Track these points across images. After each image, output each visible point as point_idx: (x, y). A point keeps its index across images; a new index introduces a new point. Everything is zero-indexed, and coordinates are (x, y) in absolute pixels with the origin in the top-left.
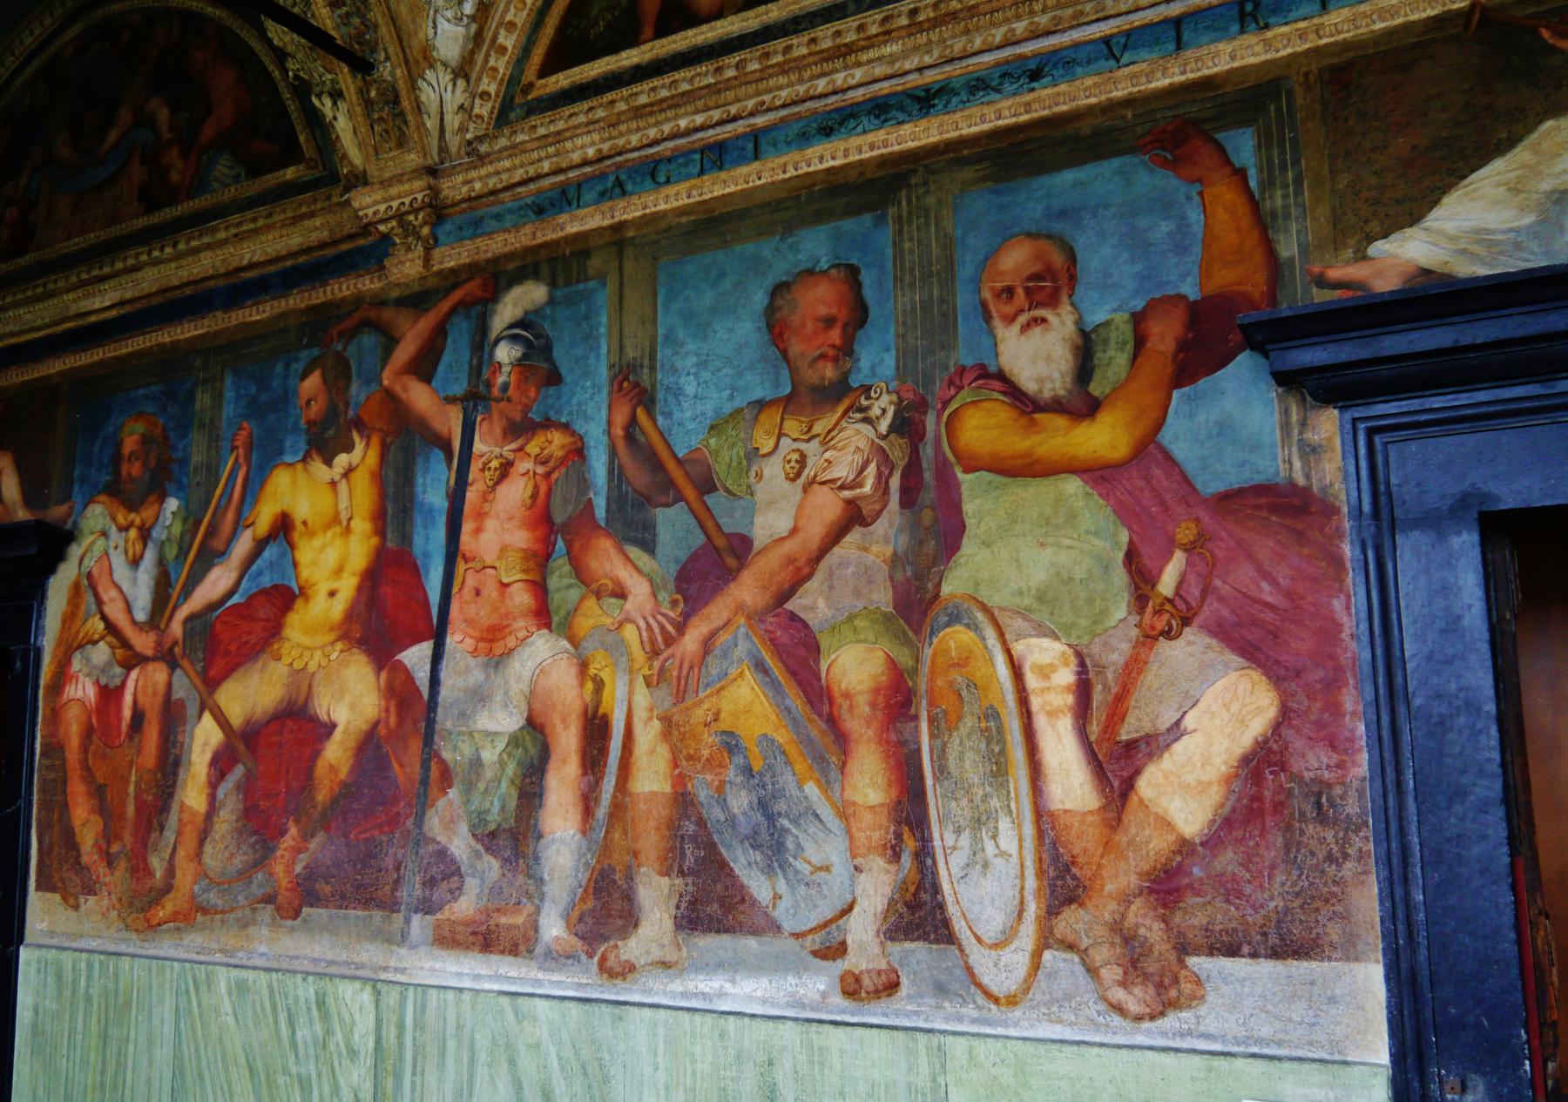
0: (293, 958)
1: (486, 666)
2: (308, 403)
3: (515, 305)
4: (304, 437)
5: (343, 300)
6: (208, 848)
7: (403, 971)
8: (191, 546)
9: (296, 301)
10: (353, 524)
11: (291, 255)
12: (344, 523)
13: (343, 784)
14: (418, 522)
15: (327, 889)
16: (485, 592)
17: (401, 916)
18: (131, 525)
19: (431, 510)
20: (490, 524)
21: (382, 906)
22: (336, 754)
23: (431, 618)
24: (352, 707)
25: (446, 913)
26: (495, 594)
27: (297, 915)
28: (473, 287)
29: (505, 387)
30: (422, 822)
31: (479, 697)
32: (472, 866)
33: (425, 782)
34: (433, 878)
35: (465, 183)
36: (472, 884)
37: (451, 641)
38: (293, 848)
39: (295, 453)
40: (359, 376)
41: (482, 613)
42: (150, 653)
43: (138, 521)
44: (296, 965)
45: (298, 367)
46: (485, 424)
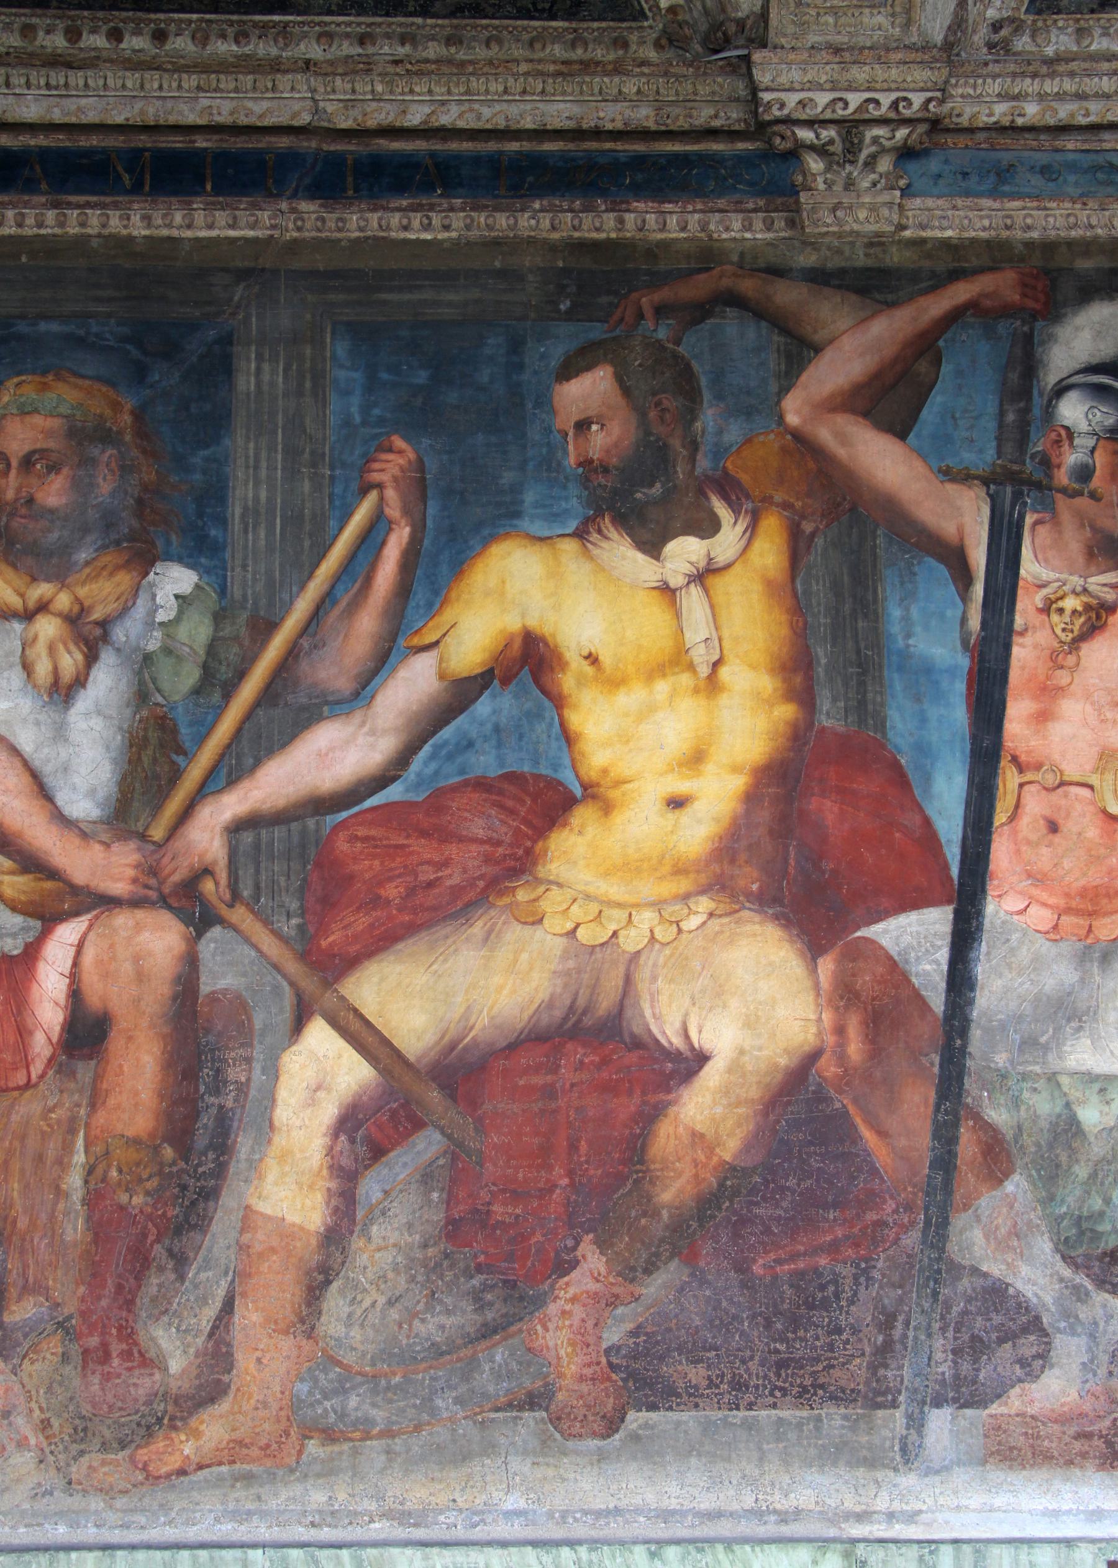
0: (598, 1514)
1: (1082, 958)
2: (583, 426)
3: (1098, 335)
4: (574, 489)
5: (665, 245)
6: (335, 1303)
7: (912, 1517)
8: (241, 675)
9: (539, 221)
10: (724, 672)
11: (541, 134)
12: (704, 671)
13: (731, 1170)
14: (897, 683)
15: (697, 1374)
16: (1070, 827)
17: (899, 1414)
18: (43, 607)
19: (928, 669)
20: (1072, 709)
21: (840, 1397)
22: (708, 1115)
23: (946, 867)
24: (750, 1023)
25: (1014, 1402)
26: (1093, 833)
27: (612, 1424)
28: (1002, 285)
29: (1084, 473)
30: (944, 1238)
31: (1069, 1013)
32: (1066, 1314)
33: (945, 1162)
34: (974, 1338)
35: (1004, 96)
36: (1070, 1349)
37: (999, 907)
38: (595, 1296)
39: (555, 517)
40: (719, 397)
41: (1067, 864)
42: (119, 888)
43: (63, 601)
44: (614, 1528)
45: (558, 352)
46: (1042, 530)
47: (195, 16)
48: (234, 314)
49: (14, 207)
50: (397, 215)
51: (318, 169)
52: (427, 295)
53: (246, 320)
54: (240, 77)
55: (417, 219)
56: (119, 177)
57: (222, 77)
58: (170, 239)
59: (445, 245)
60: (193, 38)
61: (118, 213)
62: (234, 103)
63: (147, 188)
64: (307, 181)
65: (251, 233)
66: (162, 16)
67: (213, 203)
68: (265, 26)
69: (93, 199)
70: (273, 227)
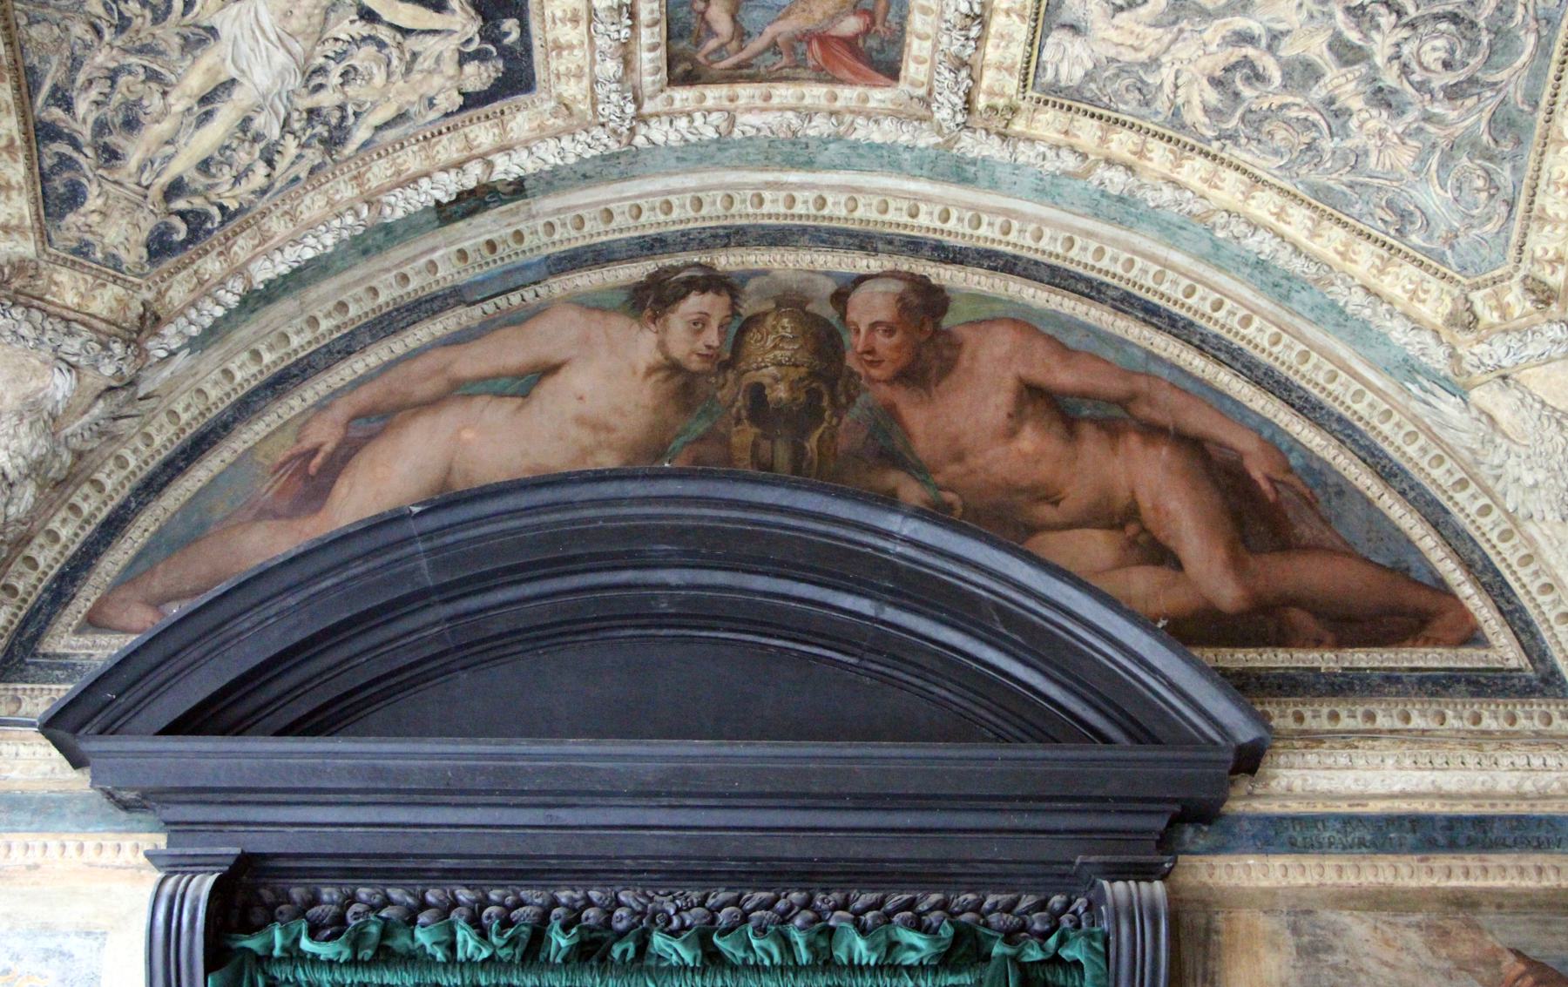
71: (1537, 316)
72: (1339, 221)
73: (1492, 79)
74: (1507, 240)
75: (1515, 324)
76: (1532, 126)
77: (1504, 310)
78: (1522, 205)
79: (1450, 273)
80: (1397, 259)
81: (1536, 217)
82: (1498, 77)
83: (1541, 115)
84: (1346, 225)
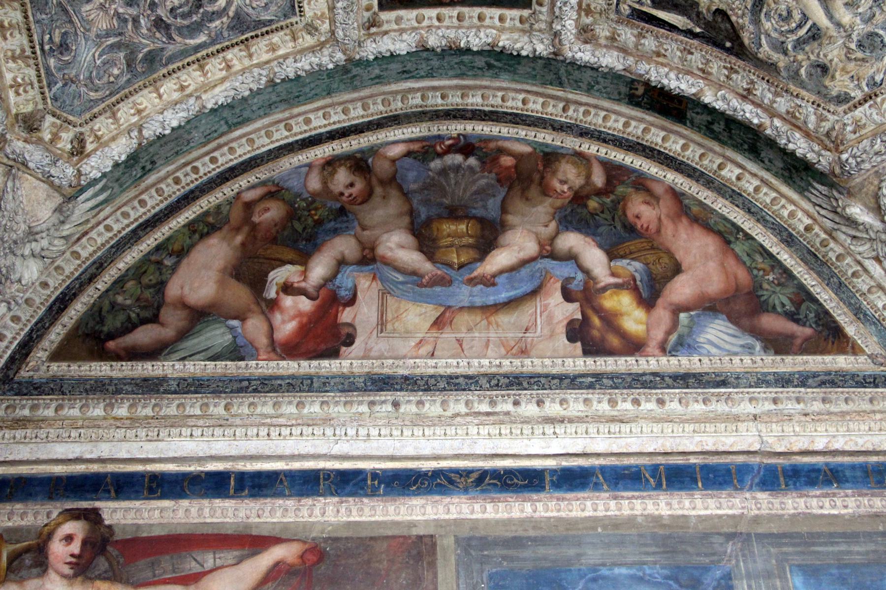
47: (677, 391)
48: (730, 560)
49: (591, 500)
50: (815, 500)
51: (762, 473)
52: (843, 548)
53: (737, 565)
54: (718, 425)
55: (827, 502)
56: (647, 480)
57: (707, 425)
58: (683, 516)
59: (847, 517)
60: (680, 402)
61: (651, 502)
62: (715, 439)
63: (664, 486)
64: (757, 480)
65: (730, 512)
66: (659, 391)
67: (706, 495)
68: (719, 394)
69: (636, 494)
70: (743, 508)
71: (66, 155)
72: (25, 12)
73: (173, 35)
74: (91, 108)
75: (54, 149)
76: (155, 71)
77: (55, 138)
78: (114, 99)
79: (47, 94)
80: (32, 62)
81: (112, 111)
82: (176, 38)
83: (165, 71)
84: (26, 17)
